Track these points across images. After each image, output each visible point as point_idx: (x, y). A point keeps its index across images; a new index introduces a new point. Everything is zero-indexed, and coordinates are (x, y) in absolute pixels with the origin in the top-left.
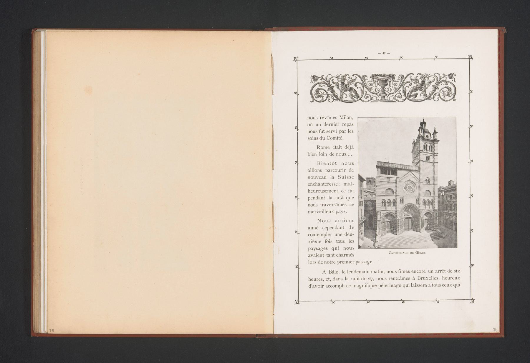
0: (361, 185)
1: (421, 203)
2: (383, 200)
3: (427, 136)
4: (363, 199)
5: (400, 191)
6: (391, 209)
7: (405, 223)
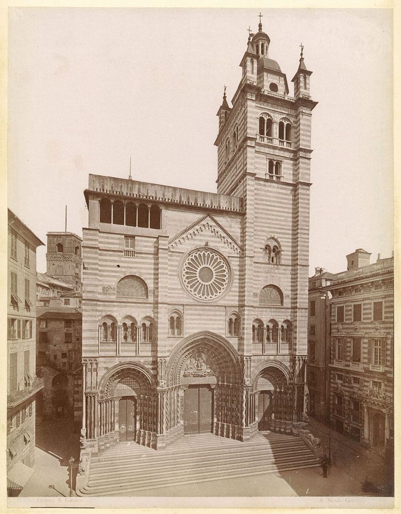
0: (27, 260)
1: (248, 333)
2: (110, 316)
3: (274, 87)
4: (33, 314)
5: (172, 287)
6: (136, 353)
7: (185, 406)
